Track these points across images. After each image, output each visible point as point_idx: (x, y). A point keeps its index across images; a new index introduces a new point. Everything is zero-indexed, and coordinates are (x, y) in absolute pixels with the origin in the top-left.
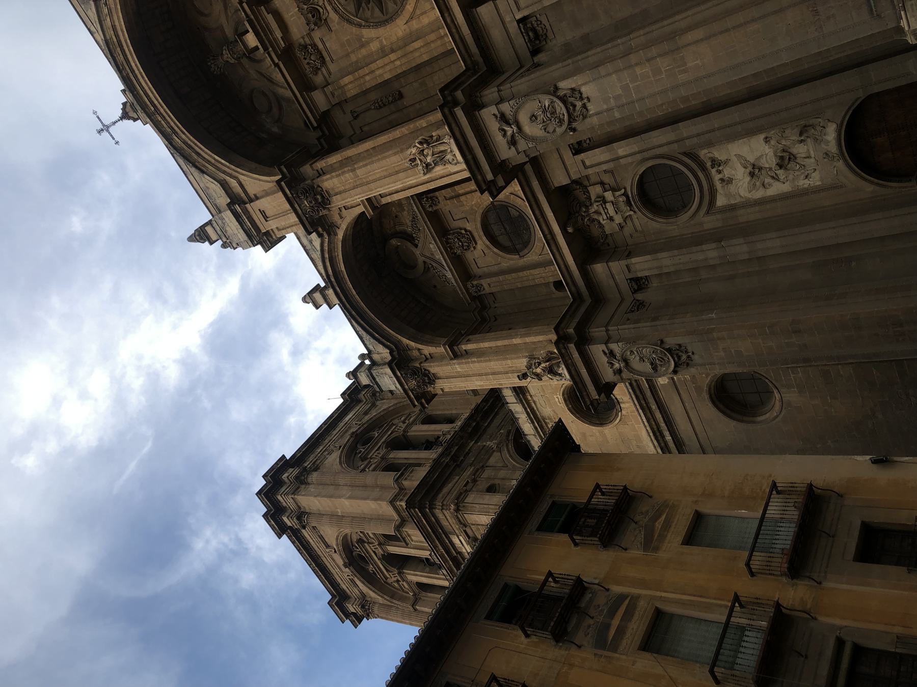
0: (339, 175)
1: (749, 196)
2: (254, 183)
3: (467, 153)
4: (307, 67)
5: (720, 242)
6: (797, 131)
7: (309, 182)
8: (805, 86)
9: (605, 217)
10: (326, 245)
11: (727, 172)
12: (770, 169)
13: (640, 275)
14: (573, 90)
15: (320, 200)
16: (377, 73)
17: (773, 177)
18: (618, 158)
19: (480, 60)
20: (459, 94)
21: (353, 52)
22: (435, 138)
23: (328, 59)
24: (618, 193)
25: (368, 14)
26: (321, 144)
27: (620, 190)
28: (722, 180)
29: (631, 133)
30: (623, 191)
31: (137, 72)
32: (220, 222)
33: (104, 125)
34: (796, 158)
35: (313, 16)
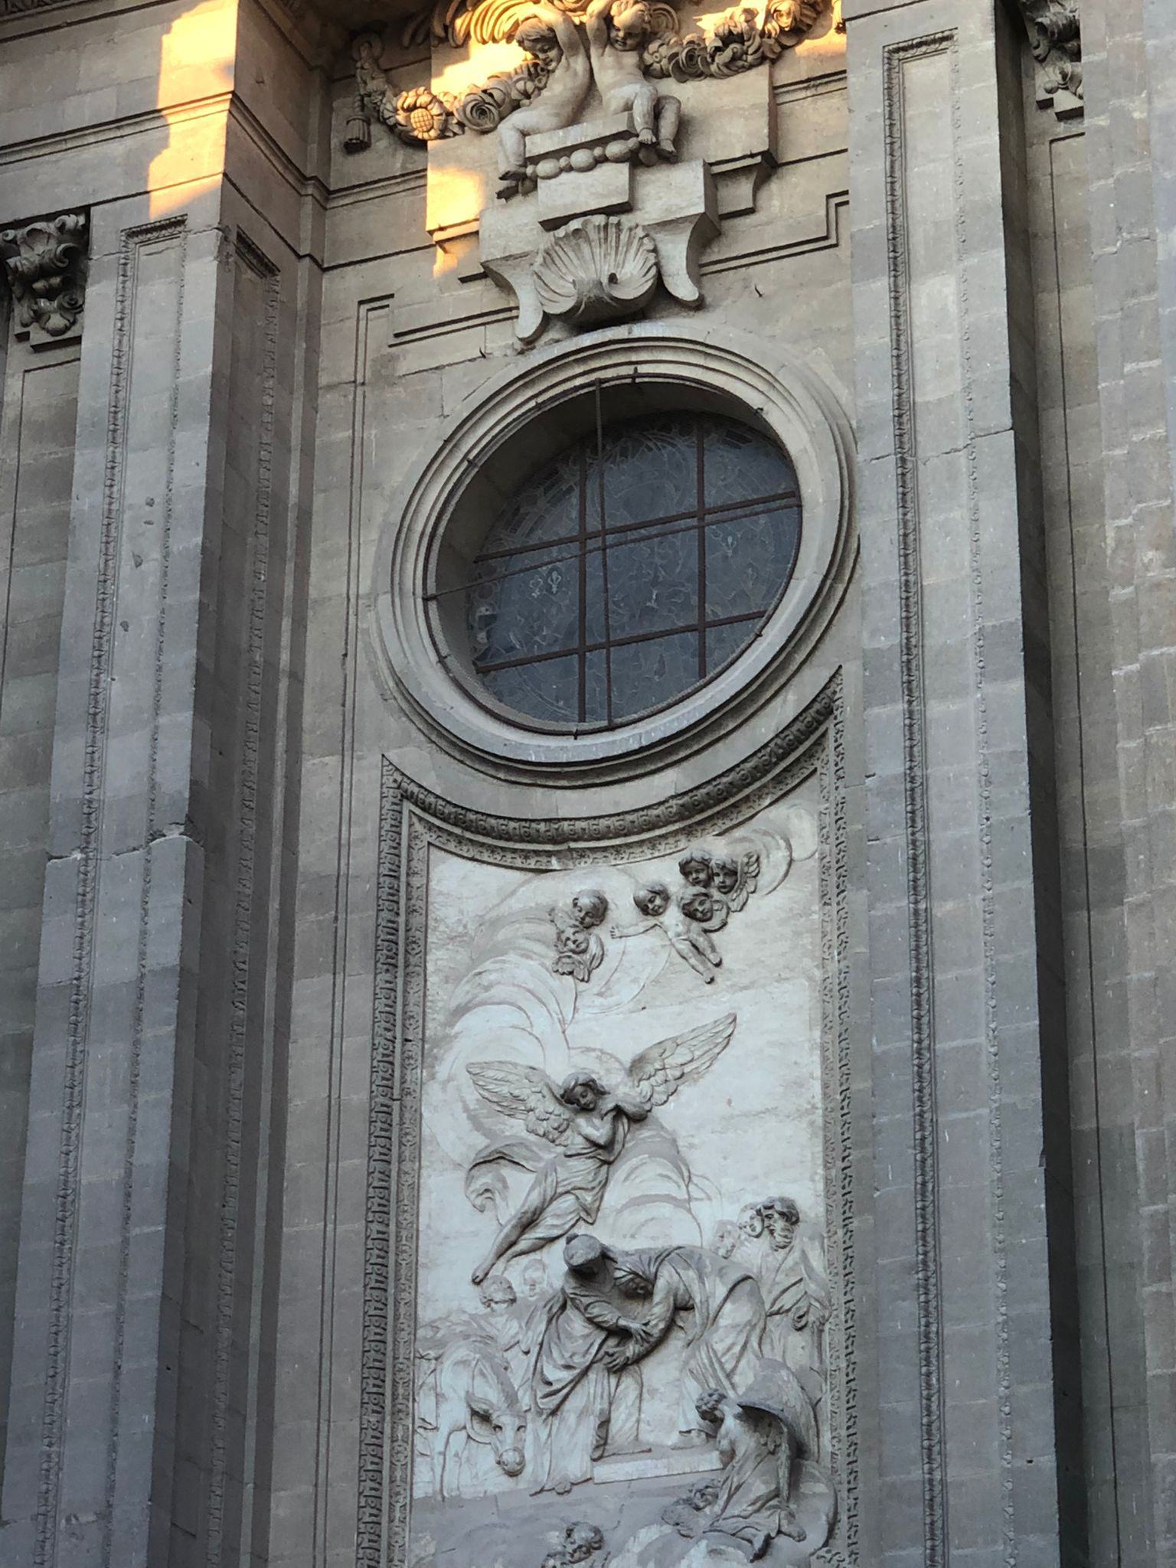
1: (452, 1063)
5: (191, 825)
6: (785, 1397)
8: (1048, 1461)
9: (539, 144)
11: (636, 951)
12: (588, 1214)
13: (99, 295)
17: (529, 1222)
18: (898, 263)
24: (676, 251)
27: (697, 270)
28: (596, 913)
29: (1036, 384)
30: (683, 288)
34: (619, 1370)
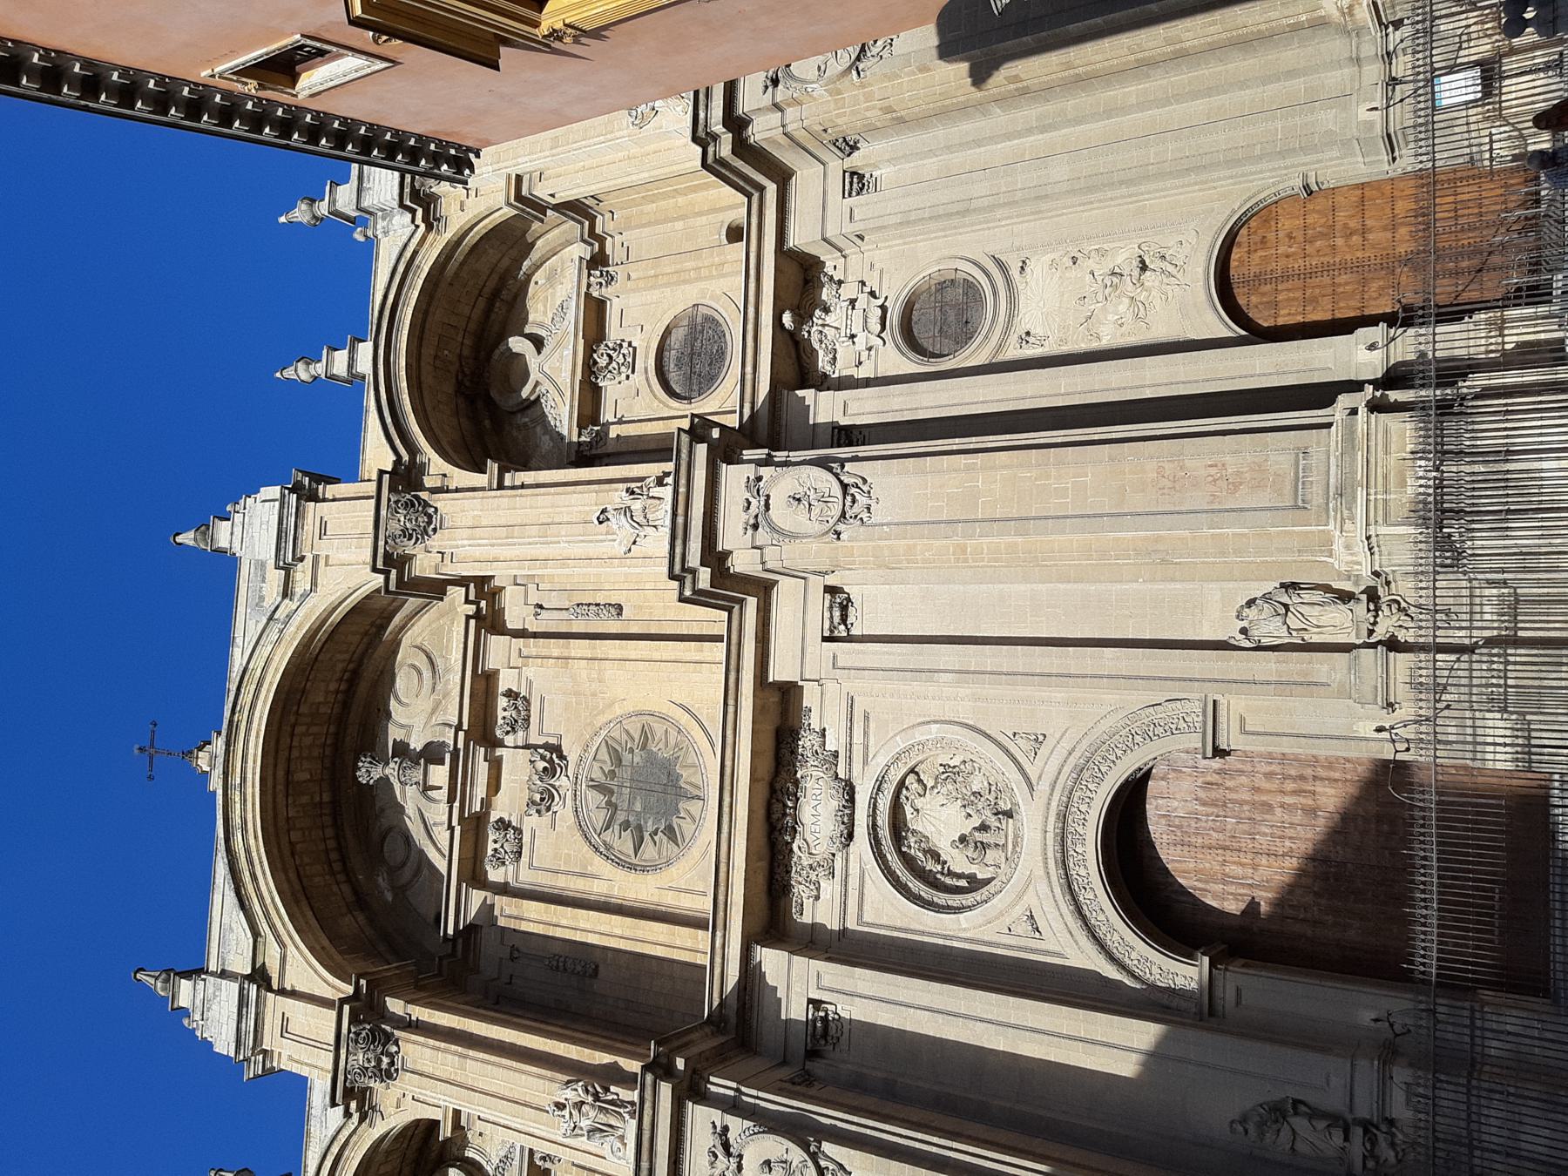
0: (438, 1049)
2: (302, 968)
3: (645, 1156)
4: (490, 852)
7: (388, 1028)
10: (345, 1133)
14: (841, 1166)
15: (384, 1066)
16: (582, 925)
19: (733, 1020)
20: (680, 1063)
21: (566, 873)
22: (610, 1097)
23: (525, 859)
25: (616, 844)
26: (440, 964)
31: (255, 725)
32: (210, 990)
33: (152, 746)
35: (542, 800)
